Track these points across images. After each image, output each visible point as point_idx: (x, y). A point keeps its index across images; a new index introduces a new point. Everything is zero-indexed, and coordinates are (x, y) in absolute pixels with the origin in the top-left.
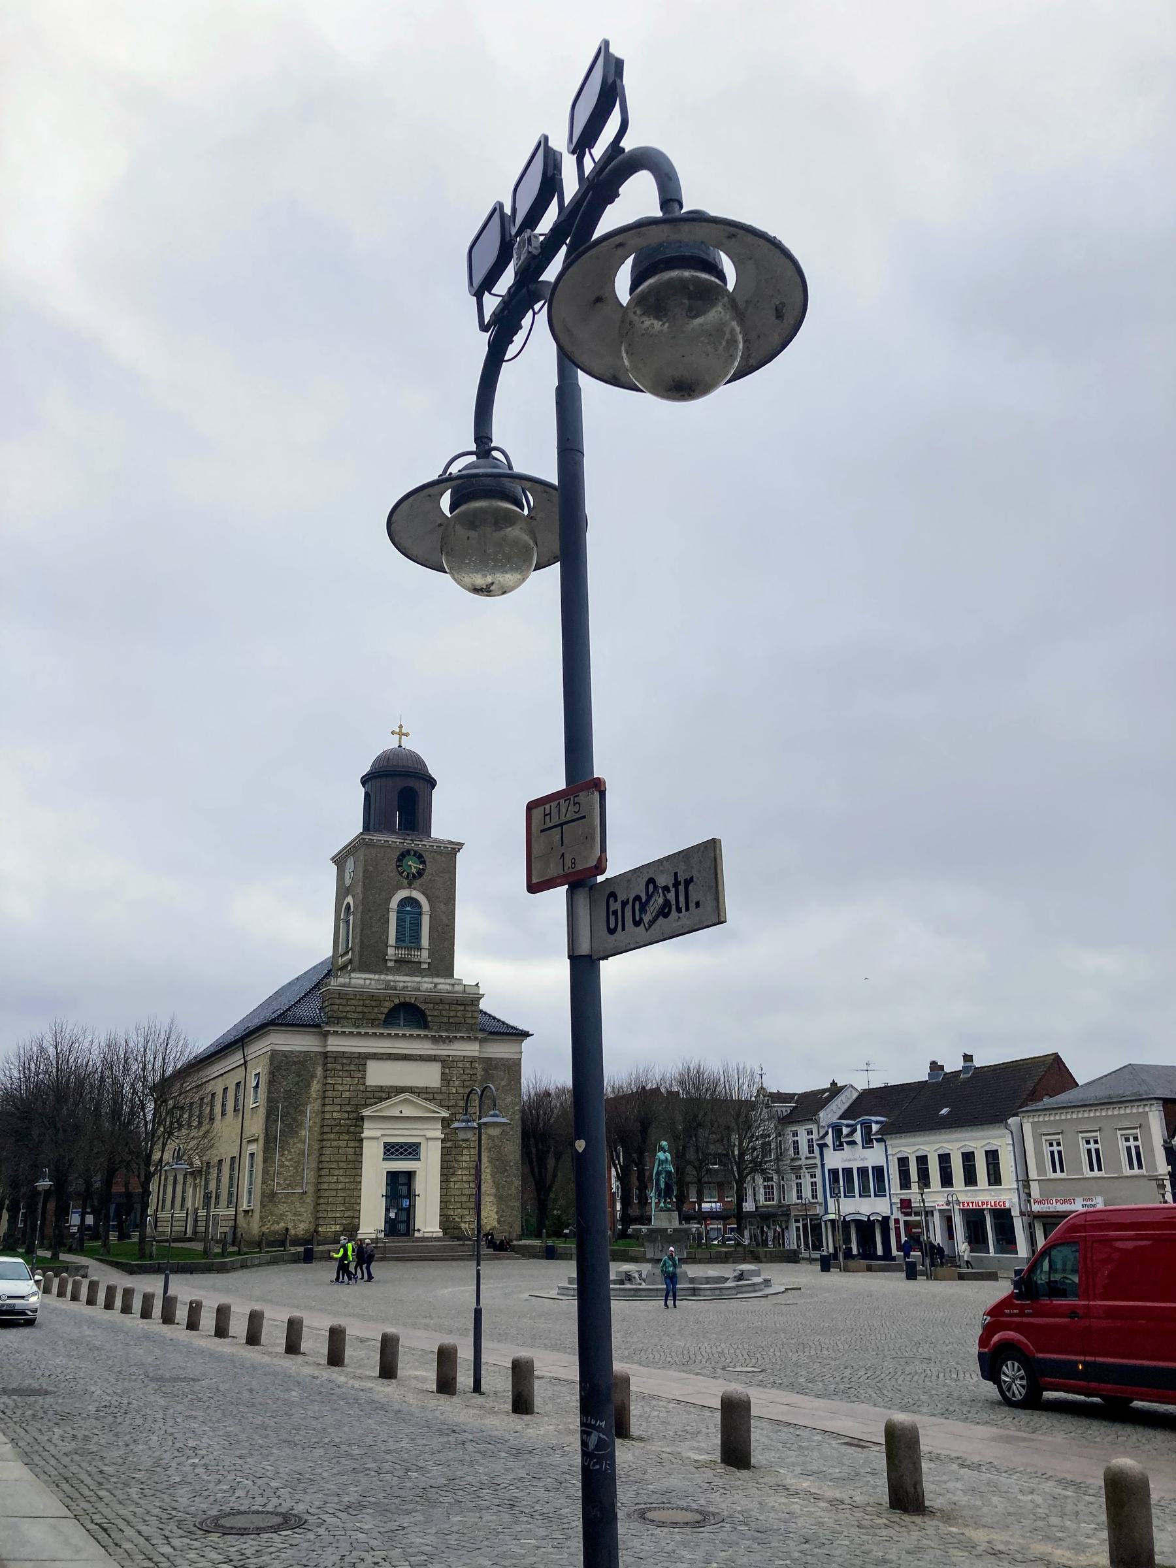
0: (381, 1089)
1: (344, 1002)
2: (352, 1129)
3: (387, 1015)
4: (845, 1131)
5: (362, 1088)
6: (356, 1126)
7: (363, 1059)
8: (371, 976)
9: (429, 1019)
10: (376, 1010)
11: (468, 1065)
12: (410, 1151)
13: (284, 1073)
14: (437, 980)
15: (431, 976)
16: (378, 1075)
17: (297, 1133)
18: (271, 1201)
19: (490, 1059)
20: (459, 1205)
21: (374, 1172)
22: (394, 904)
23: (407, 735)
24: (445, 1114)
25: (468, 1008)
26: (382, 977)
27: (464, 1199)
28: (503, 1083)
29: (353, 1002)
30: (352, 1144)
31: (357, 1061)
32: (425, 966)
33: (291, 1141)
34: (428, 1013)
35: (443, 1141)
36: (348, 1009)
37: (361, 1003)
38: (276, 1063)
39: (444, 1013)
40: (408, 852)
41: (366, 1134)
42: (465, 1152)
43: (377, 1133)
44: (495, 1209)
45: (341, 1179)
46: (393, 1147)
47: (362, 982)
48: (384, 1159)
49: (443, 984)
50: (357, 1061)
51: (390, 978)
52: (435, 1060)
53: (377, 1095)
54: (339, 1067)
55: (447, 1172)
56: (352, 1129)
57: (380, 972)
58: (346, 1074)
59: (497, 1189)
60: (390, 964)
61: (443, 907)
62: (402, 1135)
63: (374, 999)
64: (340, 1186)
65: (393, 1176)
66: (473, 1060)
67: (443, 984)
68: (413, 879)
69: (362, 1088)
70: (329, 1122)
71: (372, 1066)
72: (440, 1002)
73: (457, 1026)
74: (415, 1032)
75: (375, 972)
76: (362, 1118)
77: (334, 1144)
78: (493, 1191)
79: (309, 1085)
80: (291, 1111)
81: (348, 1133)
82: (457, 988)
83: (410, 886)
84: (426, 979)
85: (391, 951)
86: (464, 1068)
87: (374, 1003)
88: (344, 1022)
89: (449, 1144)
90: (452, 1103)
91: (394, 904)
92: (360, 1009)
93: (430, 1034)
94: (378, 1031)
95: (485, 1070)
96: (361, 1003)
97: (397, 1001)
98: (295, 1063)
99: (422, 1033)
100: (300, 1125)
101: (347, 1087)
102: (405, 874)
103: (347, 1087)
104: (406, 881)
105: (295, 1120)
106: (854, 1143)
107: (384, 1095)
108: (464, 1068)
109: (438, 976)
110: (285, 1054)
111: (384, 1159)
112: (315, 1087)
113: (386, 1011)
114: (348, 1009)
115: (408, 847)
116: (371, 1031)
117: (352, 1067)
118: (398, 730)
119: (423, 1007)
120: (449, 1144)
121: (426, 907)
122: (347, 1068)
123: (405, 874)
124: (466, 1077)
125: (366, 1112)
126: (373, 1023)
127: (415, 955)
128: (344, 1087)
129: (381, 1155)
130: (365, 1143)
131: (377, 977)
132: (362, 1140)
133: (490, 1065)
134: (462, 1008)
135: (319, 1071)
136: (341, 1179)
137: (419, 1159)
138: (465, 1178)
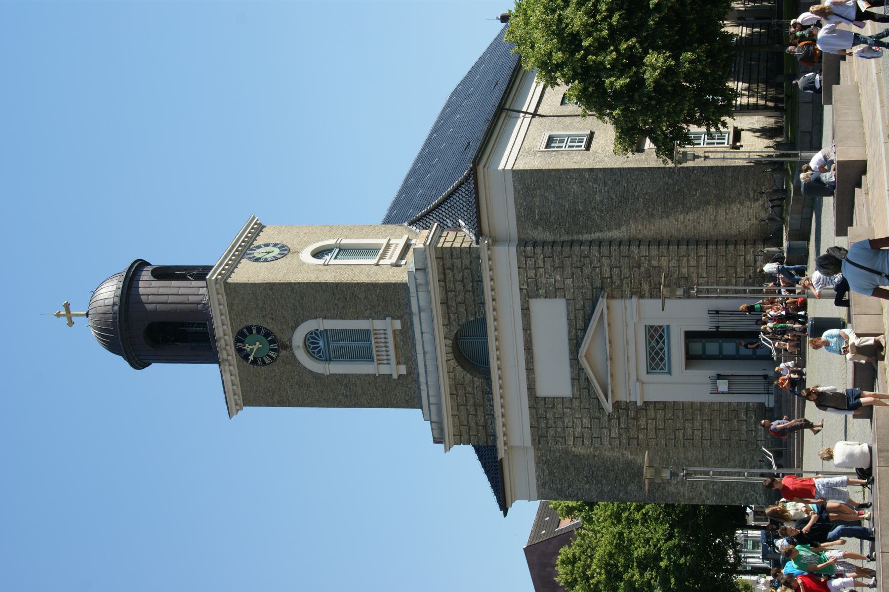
1: (464, 429)
2: (632, 414)
6: (627, 409)
7: (539, 405)
9: (472, 319)
10: (469, 389)
11: (530, 262)
12: (656, 336)
14: (415, 308)
15: (411, 314)
18: (726, 495)
19: (518, 218)
20: (731, 271)
21: (688, 385)
22: (317, 367)
23: (67, 306)
25: (448, 265)
26: (422, 379)
27: (722, 263)
28: (552, 197)
29: (463, 418)
30: (651, 413)
32: (398, 325)
35: (642, 297)
36: (472, 424)
39: (460, 299)
42: (655, 263)
44: (735, 207)
45: (697, 424)
46: (653, 359)
52: (528, 309)
53: (583, 383)
54: (552, 432)
55: (686, 287)
56: (632, 414)
58: (560, 424)
59: (708, 203)
60: (403, 369)
62: (636, 350)
64: (706, 425)
65: (692, 359)
66: (523, 257)
69: (576, 403)
71: (544, 390)
73: (478, 281)
77: (652, 434)
78: (711, 209)
81: (636, 418)
86: (536, 269)
89: (646, 287)
90: (587, 283)
91: (317, 367)
92: (472, 410)
95: (536, 225)
97: (453, 362)
98: (550, 473)
101: (577, 422)
102: (273, 354)
103: (577, 422)
104: (283, 353)
107: (582, 376)
108: (536, 269)
109: (408, 304)
111: (669, 373)
112: (580, 450)
114: (472, 424)
115: (232, 350)
117: (550, 415)
118: (65, 320)
119: (455, 329)
120: (646, 287)
122: (551, 422)
123: (273, 354)
124: (548, 265)
129: (665, 378)
130: (651, 398)
131: (423, 387)
132: (645, 403)
133: (526, 214)
134: (449, 274)
136: (697, 424)
137: (668, 327)
138: (693, 263)
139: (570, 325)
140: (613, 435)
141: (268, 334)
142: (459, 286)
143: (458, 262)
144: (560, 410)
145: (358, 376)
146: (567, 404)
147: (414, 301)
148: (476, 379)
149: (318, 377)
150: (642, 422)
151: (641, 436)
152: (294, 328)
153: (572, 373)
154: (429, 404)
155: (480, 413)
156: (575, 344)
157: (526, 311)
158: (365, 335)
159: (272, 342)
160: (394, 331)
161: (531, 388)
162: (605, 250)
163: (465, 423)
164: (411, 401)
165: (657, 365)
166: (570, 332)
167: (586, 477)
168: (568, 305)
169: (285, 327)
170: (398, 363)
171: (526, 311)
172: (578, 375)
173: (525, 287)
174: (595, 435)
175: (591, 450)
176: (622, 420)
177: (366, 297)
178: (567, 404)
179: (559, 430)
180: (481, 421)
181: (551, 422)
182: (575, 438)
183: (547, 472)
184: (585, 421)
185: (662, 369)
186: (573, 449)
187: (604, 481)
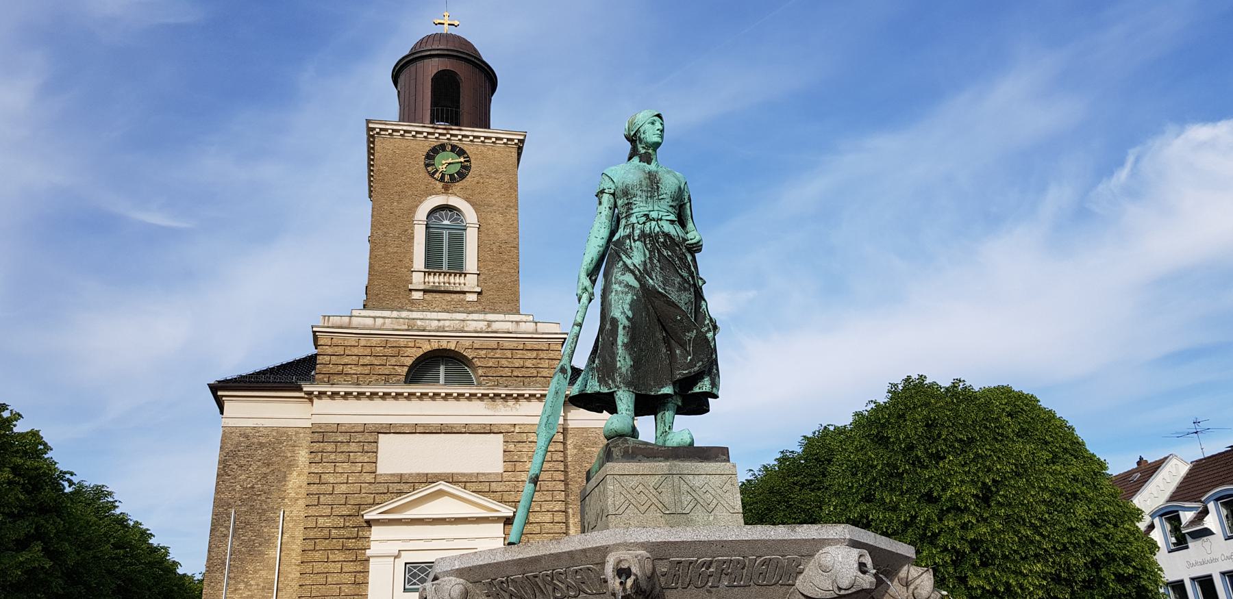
0: (401, 479)
1: (340, 350)
3: (411, 368)
4: (1186, 517)
5: (370, 478)
8: (386, 313)
10: (393, 361)
13: (242, 462)
14: (490, 317)
15: (483, 312)
16: (396, 457)
17: (261, 553)
19: (586, 429)
24: (507, 512)
25: (542, 355)
26: (404, 314)
29: (355, 351)
30: (349, 567)
31: (360, 437)
32: (474, 297)
33: (250, 567)
34: (477, 362)
36: (346, 360)
37: (368, 351)
38: (230, 447)
39: (504, 362)
40: (443, 147)
41: (374, 549)
43: (393, 548)
47: (370, 322)
48: (405, 590)
49: (502, 323)
50: (360, 437)
51: (415, 315)
54: (330, 447)
57: (401, 309)
60: (417, 295)
61: (499, 218)
63: (389, 346)
67: (502, 323)
68: (450, 181)
69: (370, 478)
70: (312, 534)
72: (498, 345)
73: (526, 380)
74: (455, 390)
75: (392, 310)
76: (369, 523)
77: (319, 567)
79: (284, 479)
80: (254, 518)
81: (344, 549)
82: (523, 327)
83: (446, 189)
84: (475, 316)
85: (418, 280)
87: (389, 351)
88: (336, 379)
92: (366, 360)
93: (479, 392)
94: (393, 390)
96: (368, 351)
97: (427, 347)
98: (261, 445)
99: (467, 391)
100: (269, 541)
104: (440, 185)
105: (259, 534)
106: (1207, 532)
107: (405, 487)
109: (494, 311)
110: (244, 434)
111: (405, 590)
112: (296, 482)
113: (409, 362)
114: (346, 360)
115: (443, 139)
116: (381, 390)
117: (353, 447)
119: (469, 354)
121: (470, 215)
122: (345, 448)
125: (371, 515)
126: (387, 379)
127: (455, 282)
128: (341, 478)
130: (373, 565)
131: (395, 314)
132: (367, 560)
135: (303, 456)
139: (471, 475)
140: (321, 520)
141: (462, 175)
142: (517, 363)
143: (545, 364)
144: (361, 459)
145: (409, 252)
146: (367, 468)
147: (501, 317)
148: (406, 369)
149: (412, 210)
150: (340, 556)
151: (317, 555)
152: (467, 200)
153: (410, 475)
154: (375, 318)
155: (360, 369)
156: (452, 479)
157: (489, 430)
158: (457, 267)
159: (451, 176)
160: (464, 293)
161: (390, 430)
162: (560, 517)
163: (347, 352)
164: (373, 300)
165: (414, 576)
166: (463, 475)
167: (252, 487)
168: (497, 474)
169: (469, 192)
170: (425, 291)
171: (489, 430)
172: (405, 484)
173: (517, 430)
174: (322, 498)
175: (293, 495)
176: (342, 532)
177: (502, 272)
178: (367, 468)
179: (333, 457)
180: (347, 369)
181: (345, 448)
182: (320, 475)
183: (263, 440)
184: (344, 488)
185: (409, 581)
186: (295, 473)
187: (244, 509)
